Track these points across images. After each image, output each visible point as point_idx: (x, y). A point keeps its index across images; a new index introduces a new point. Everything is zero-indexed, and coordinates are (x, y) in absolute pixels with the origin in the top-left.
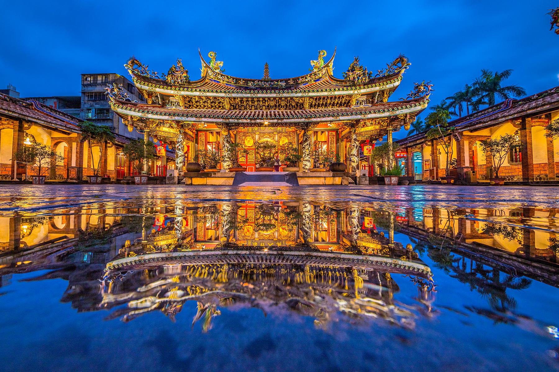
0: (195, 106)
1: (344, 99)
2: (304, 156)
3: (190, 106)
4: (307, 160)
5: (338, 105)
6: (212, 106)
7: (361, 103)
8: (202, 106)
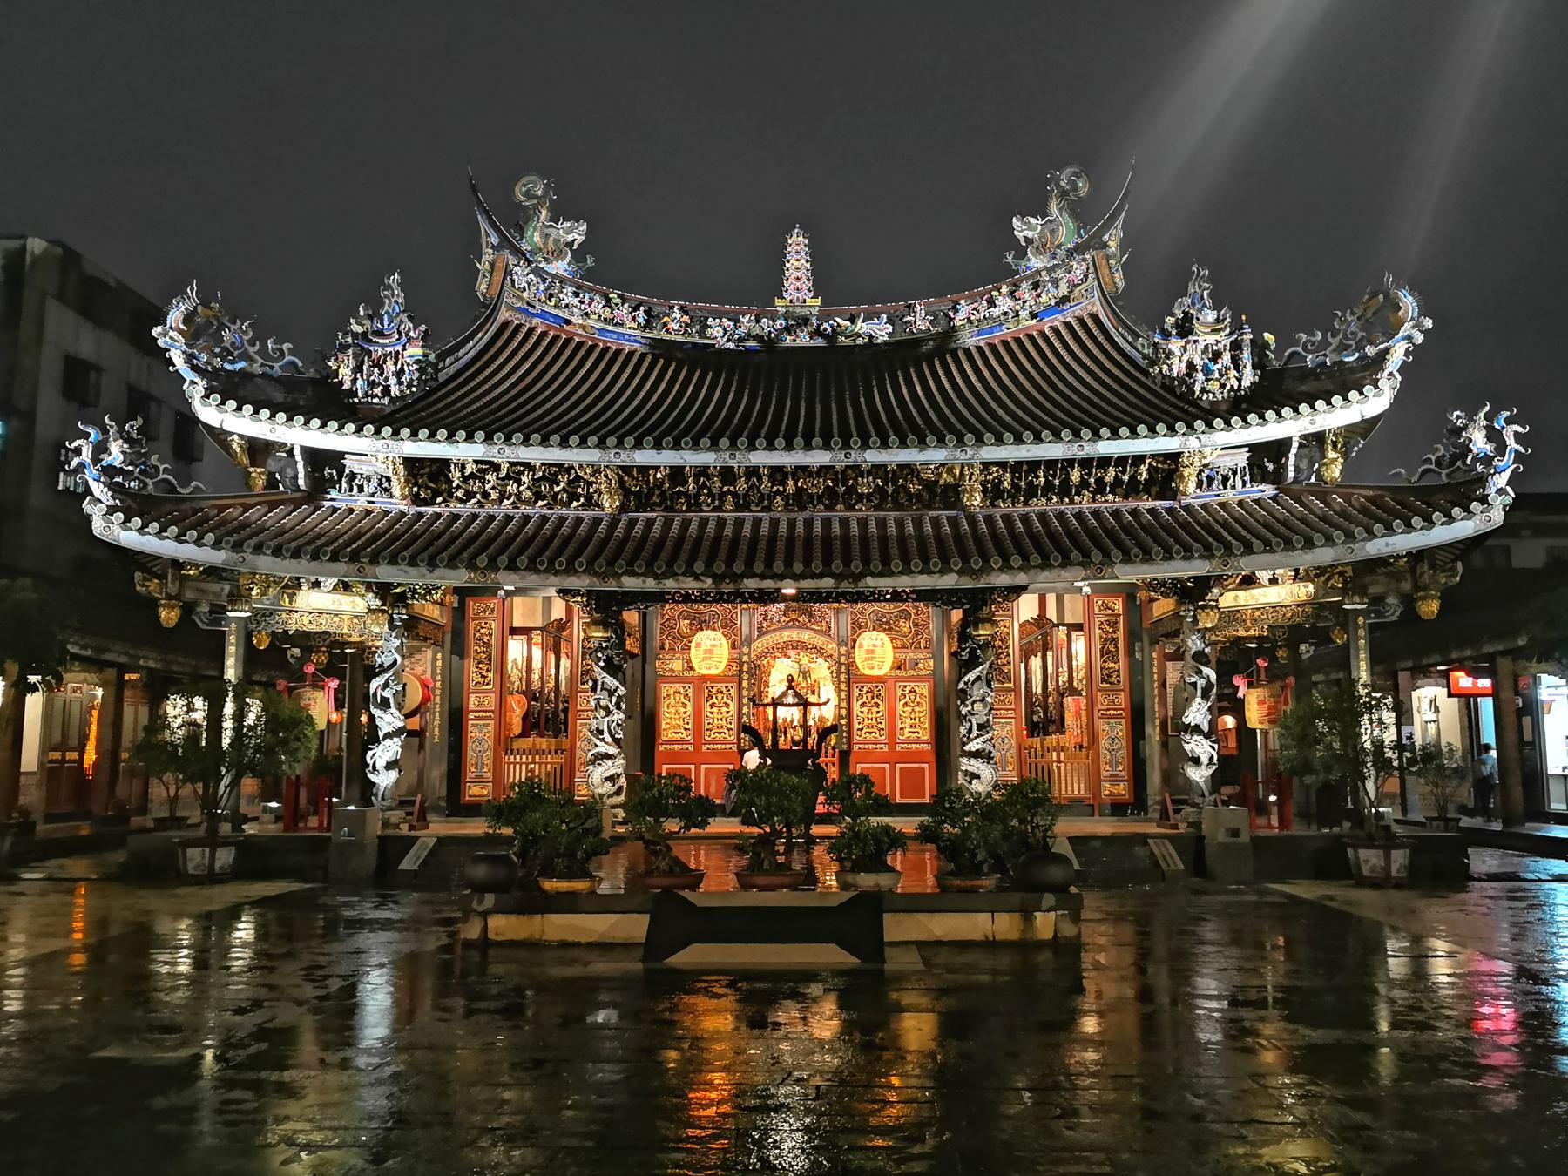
0: (460, 493)
1: (1143, 468)
2: (963, 730)
3: (436, 493)
4: (976, 755)
5: (1118, 490)
6: (539, 496)
7: (1225, 479)
8: (494, 495)
